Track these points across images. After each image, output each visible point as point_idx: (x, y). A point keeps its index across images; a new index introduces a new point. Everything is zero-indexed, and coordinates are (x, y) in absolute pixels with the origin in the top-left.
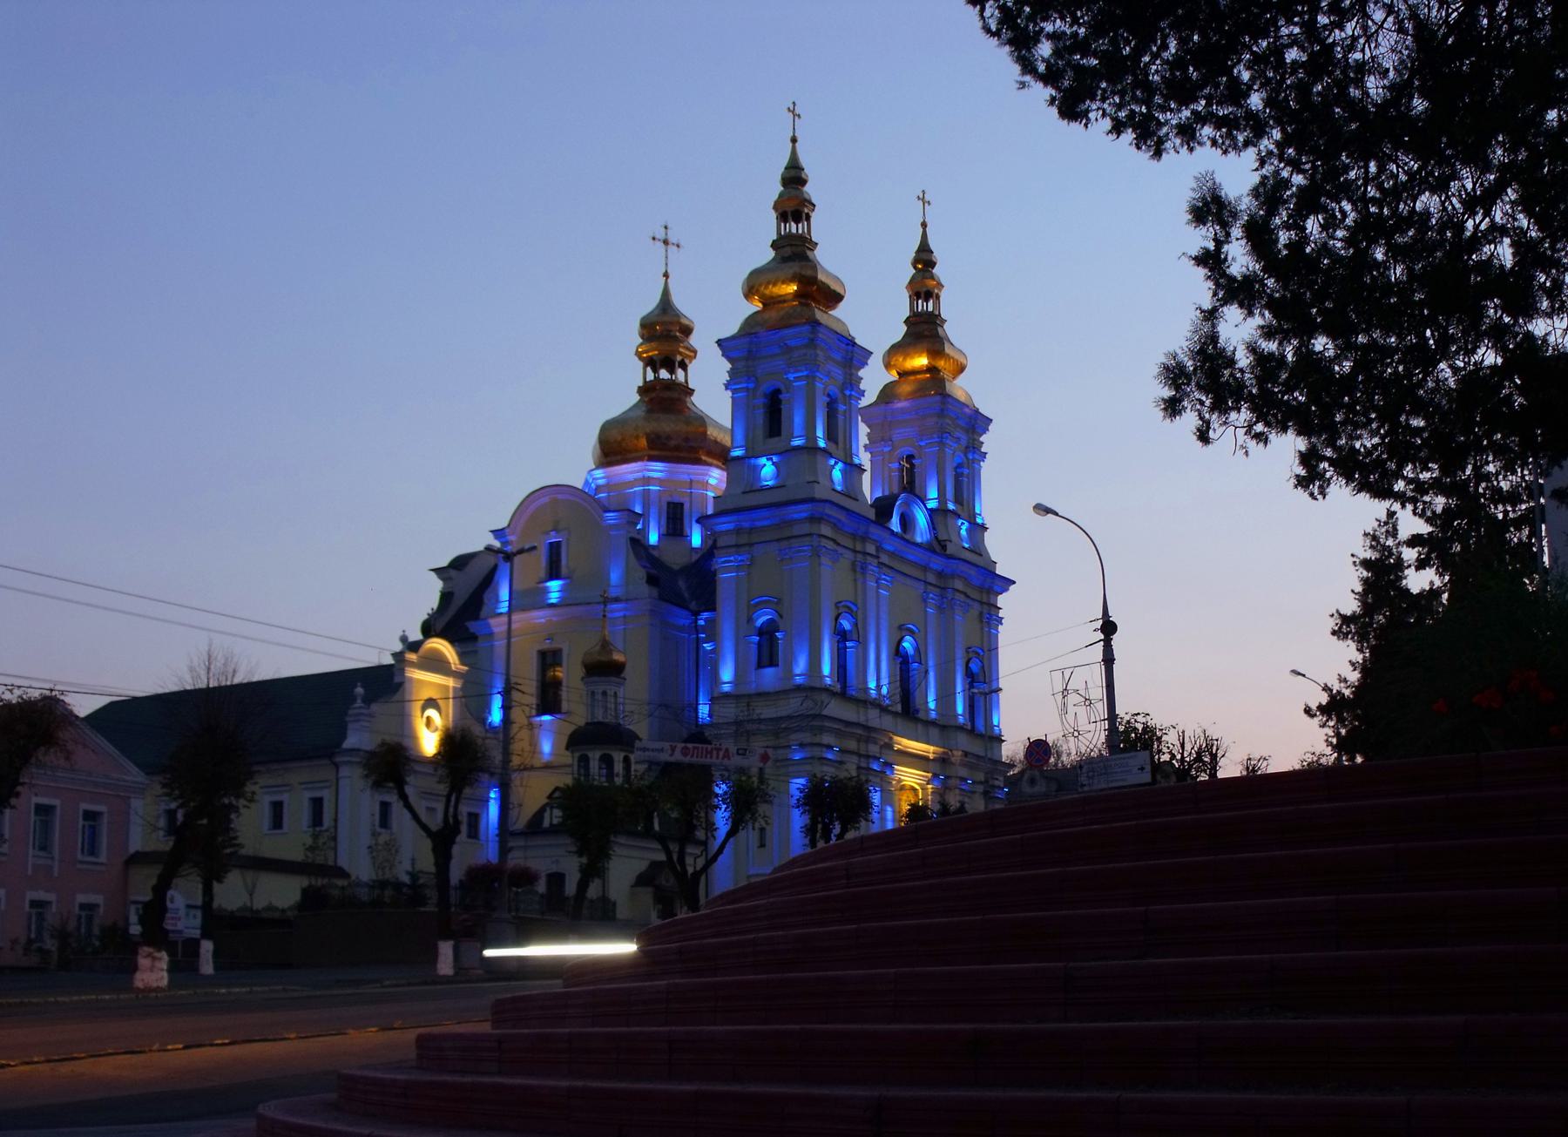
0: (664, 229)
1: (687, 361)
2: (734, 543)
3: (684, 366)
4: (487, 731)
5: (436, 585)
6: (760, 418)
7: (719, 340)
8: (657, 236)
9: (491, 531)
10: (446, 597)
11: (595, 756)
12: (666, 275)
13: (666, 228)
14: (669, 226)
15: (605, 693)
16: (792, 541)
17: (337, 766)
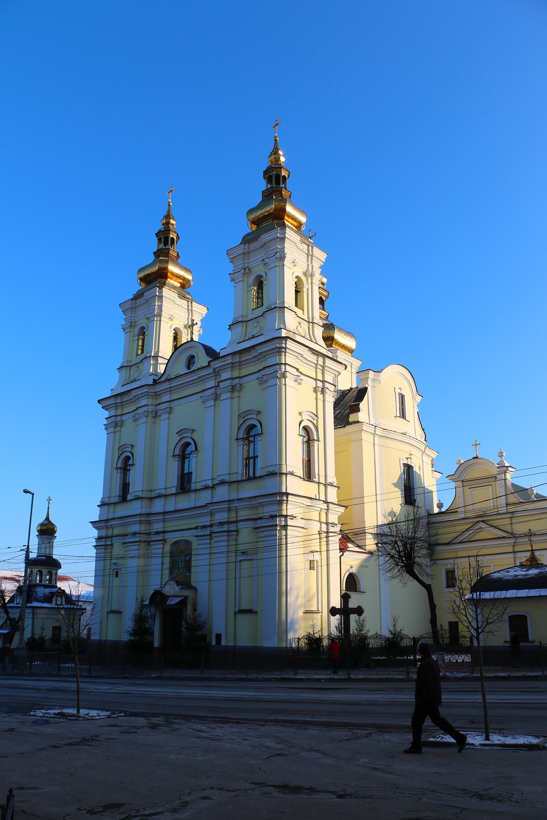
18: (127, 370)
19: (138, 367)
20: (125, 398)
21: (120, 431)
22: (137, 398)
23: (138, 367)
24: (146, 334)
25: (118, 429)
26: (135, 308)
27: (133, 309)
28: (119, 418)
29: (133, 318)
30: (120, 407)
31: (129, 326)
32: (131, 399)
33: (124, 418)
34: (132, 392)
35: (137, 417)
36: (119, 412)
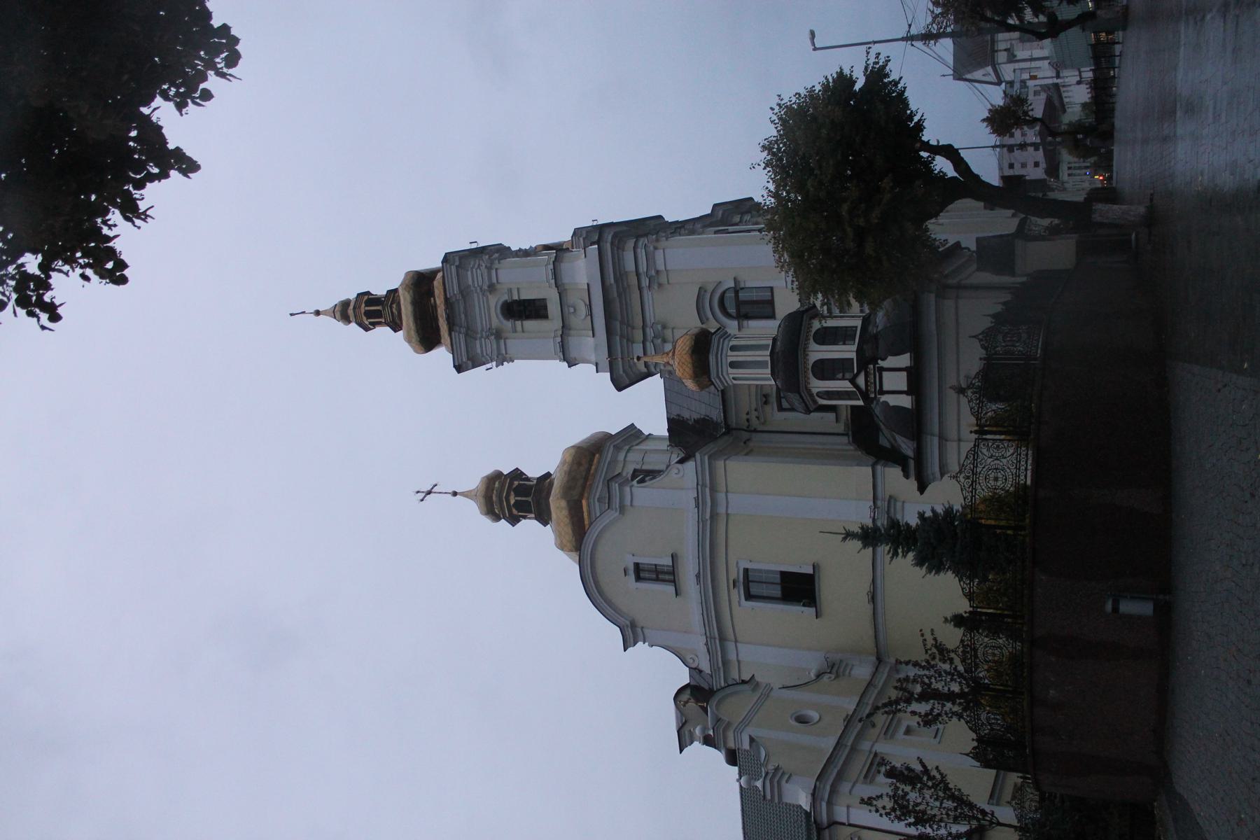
0: (419, 494)
1: (524, 476)
2: (642, 345)
3: (528, 479)
4: (830, 673)
5: (697, 748)
6: (530, 324)
7: (455, 366)
8: (421, 498)
9: (625, 650)
10: (708, 741)
11: (818, 352)
12: (455, 494)
13: (418, 492)
14: (417, 490)
15: (733, 348)
16: (641, 271)
17: (833, 823)
18: (569, 335)
19: (569, 306)
20: (617, 306)
21: (673, 329)
22: (620, 276)
23: (569, 306)
24: (516, 297)
25: (668, 333)
26: (468, 328)
27: (470, 334)
28: (650, 333)
29: (484, 333)
30: (629, 328)
31: (495, 338)
32: (619, 295)
33: (650, 318)
34: (607, 283)
35: (653, 273)
36: (638, 335)
